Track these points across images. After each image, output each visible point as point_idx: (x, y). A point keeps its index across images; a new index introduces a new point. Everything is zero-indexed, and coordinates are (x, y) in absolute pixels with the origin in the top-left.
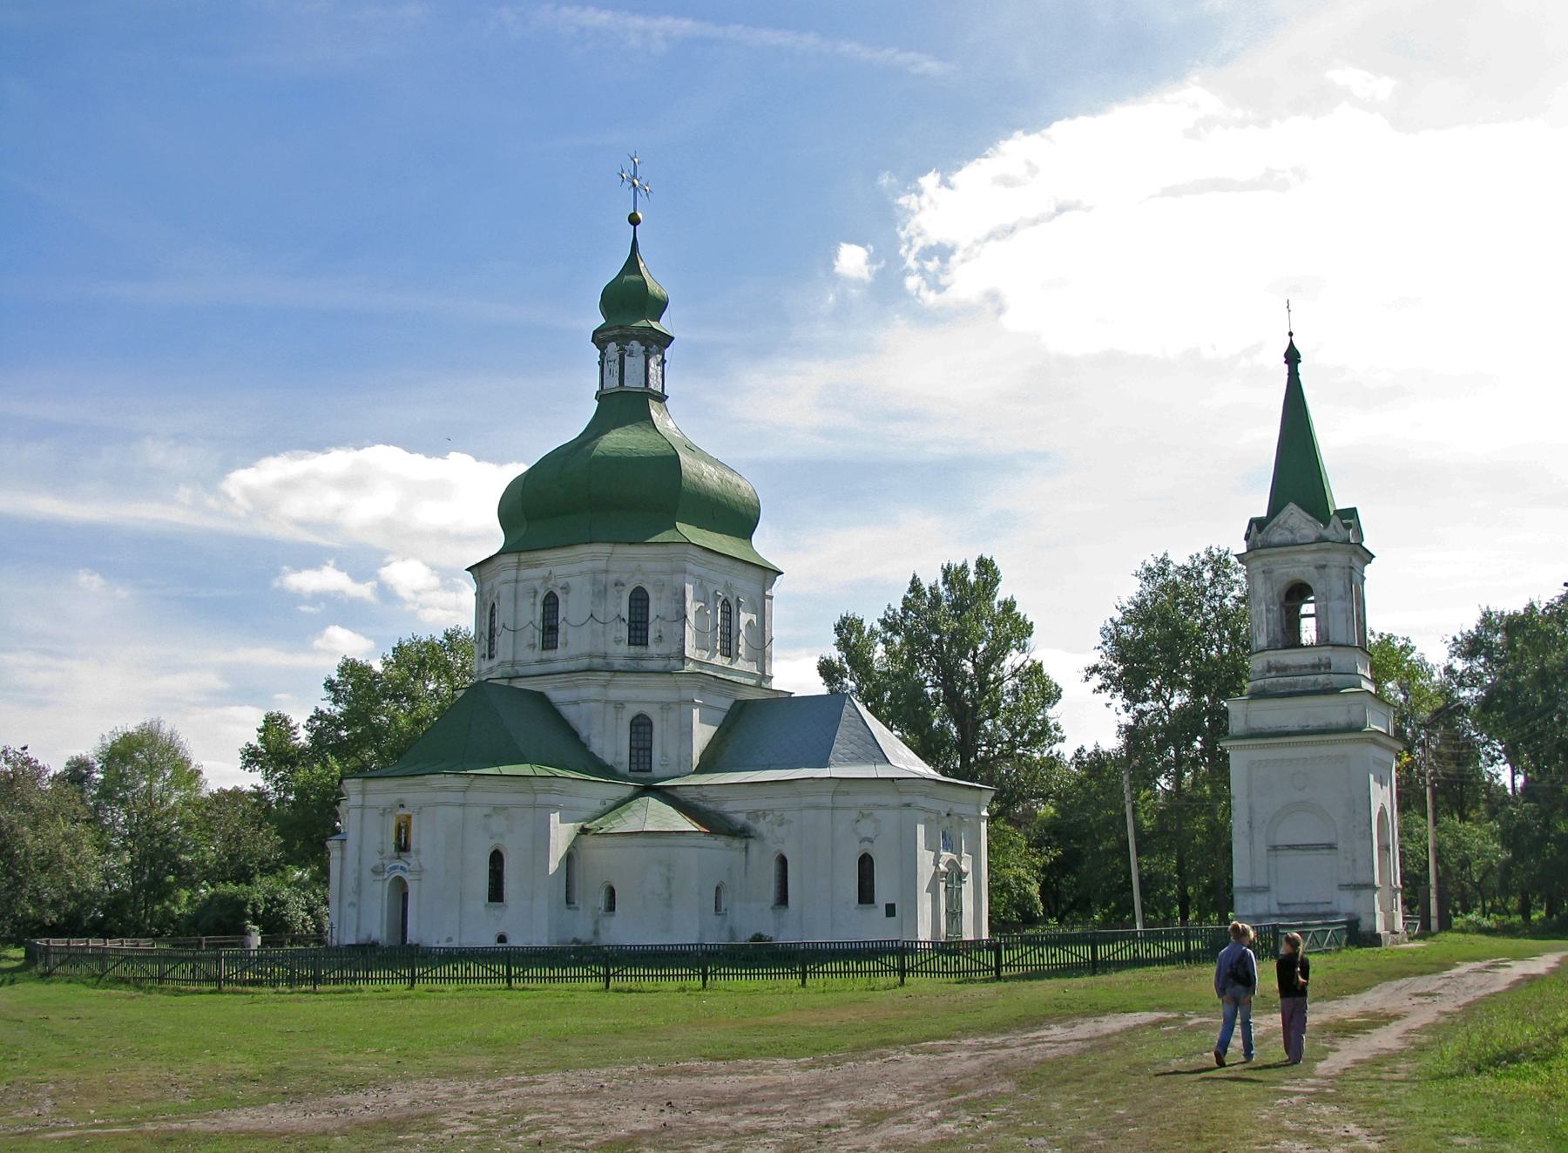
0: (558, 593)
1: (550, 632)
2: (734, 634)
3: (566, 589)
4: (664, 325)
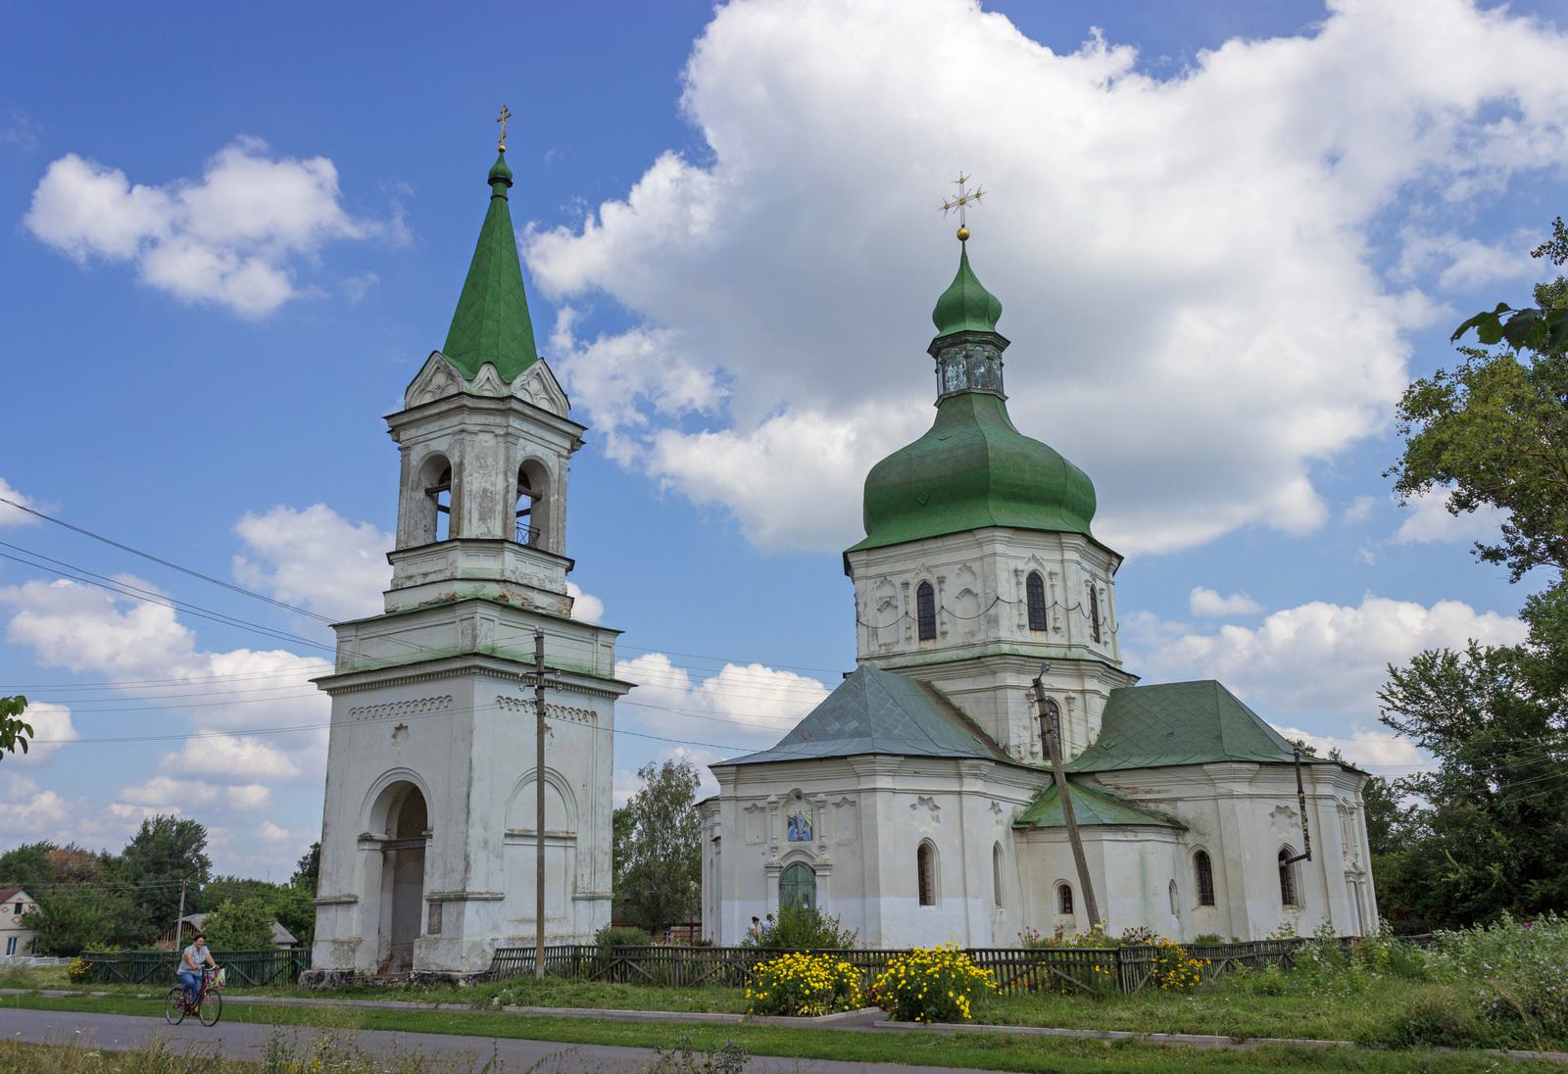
0: (934, 582)
1: (928, 627)
2: (1101, 621)
3: (941, 580)
4: (1000, 328)
